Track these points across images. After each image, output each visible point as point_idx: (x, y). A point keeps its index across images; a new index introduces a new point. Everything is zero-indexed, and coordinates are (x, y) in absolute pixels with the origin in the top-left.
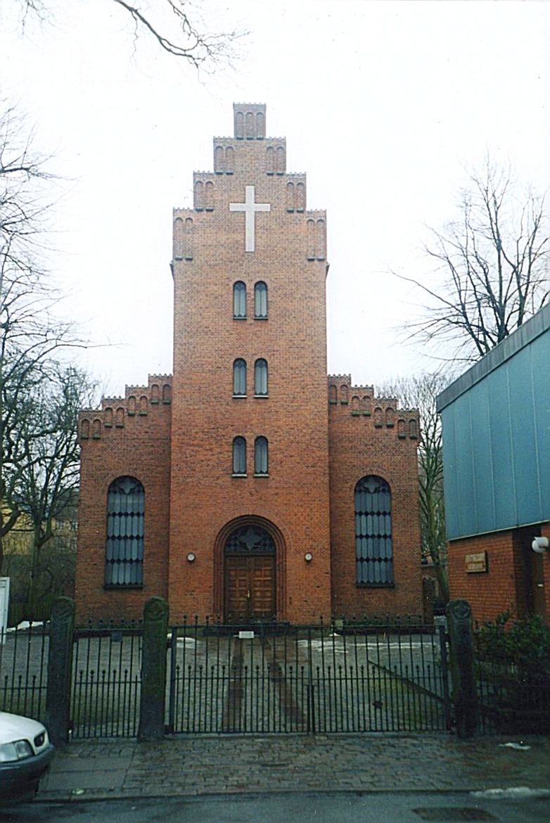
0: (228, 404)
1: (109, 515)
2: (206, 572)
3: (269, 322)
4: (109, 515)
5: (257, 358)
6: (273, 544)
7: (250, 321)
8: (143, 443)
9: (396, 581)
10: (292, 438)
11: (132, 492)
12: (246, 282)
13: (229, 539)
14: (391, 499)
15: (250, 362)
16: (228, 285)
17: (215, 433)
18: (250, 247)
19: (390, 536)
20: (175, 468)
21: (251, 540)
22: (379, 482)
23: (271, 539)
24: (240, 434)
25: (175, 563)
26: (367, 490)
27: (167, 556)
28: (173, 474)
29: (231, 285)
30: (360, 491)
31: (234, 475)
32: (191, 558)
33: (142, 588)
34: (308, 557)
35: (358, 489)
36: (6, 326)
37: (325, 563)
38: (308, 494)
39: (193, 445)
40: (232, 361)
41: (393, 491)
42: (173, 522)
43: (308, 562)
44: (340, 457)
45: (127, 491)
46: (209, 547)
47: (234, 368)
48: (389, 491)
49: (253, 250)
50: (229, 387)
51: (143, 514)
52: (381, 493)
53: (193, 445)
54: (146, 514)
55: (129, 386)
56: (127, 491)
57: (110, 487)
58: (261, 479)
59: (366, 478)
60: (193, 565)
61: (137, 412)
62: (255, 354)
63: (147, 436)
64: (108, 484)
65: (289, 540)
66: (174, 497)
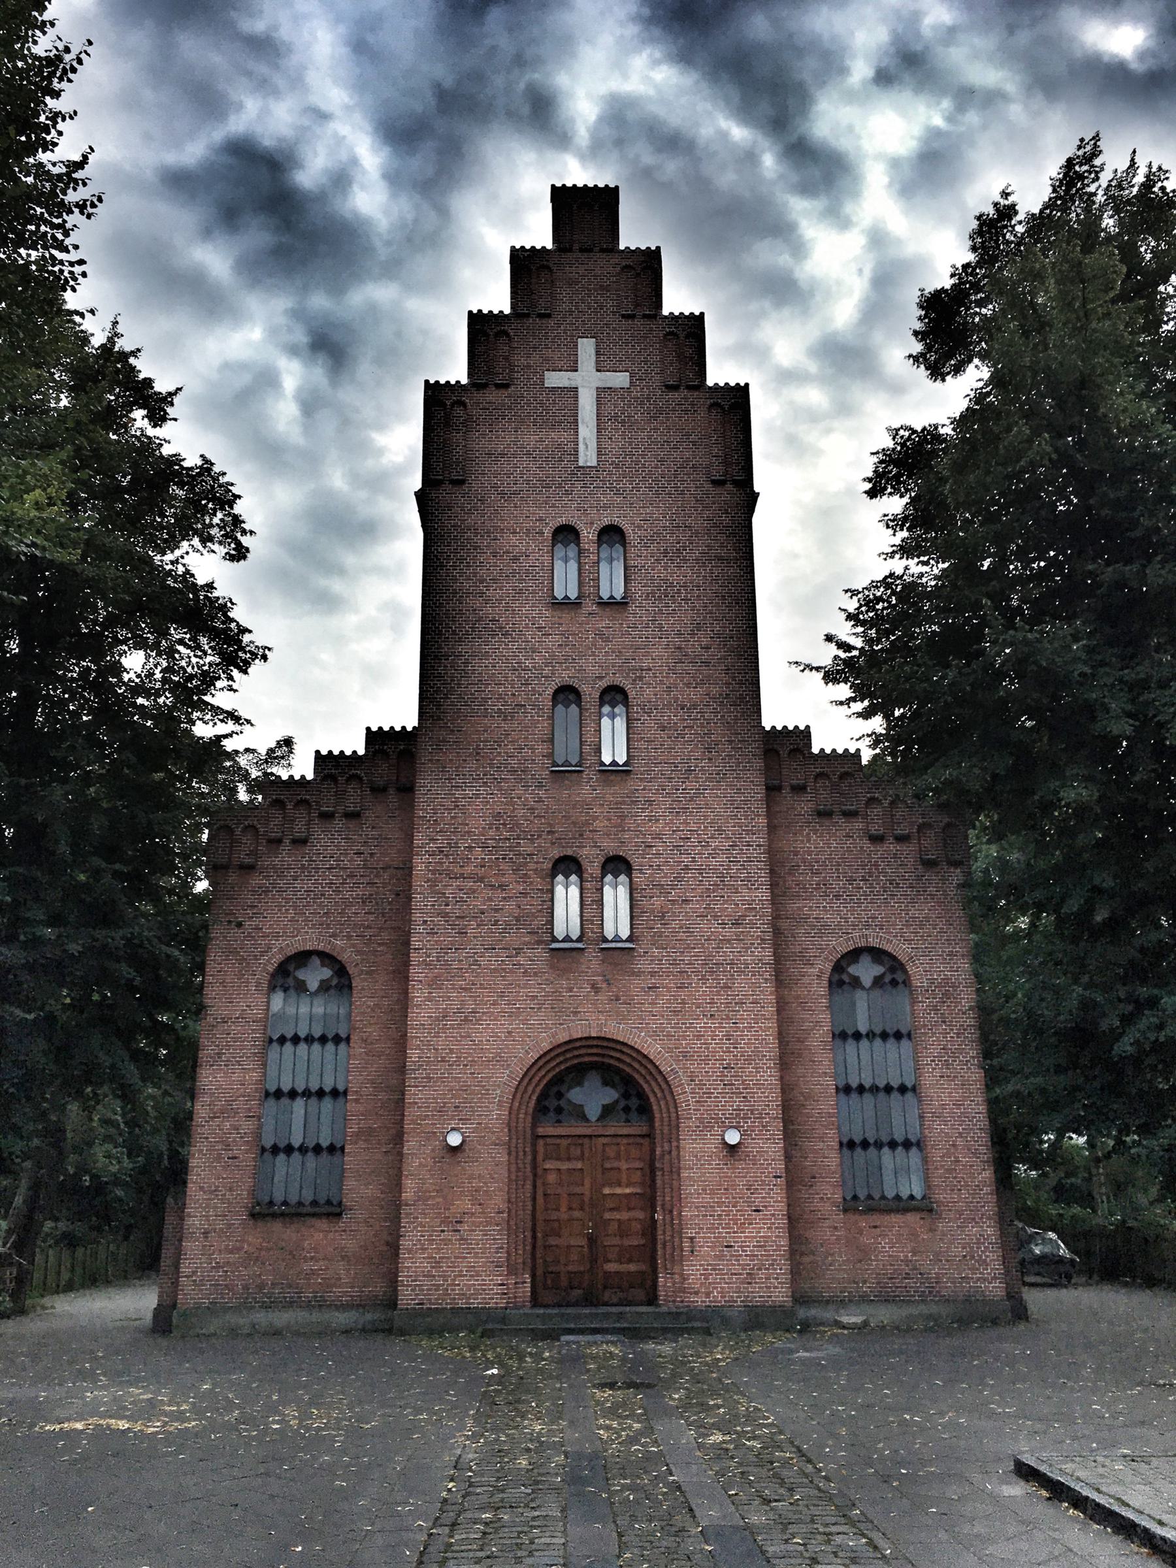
0: (540, 786)
1: (271, 1041)
2: (491, 1170)
3: (632, 608)
4: (271, 1041)
5: (603, 684)
6: (645, 1110)
7: (590, 607)
8: (351, 876)
9: (940, 1196)
10: (686, 860)
11: (325, 987)
12: (580, 526)
13: (544, 1096)
14: (914, 1002)
15: (590, 692)
16: (541, 533)
17: (511, 849)
18: (588, 456)
19: (914, 1089)
20: (421, 929)
21: (592, 1097)
22: (881, 963)
23: (642, 1096)
24: (569, 852)
25: (418, 1156)
26: (856, 983)
27: (398, 1138)
28: (415, 942)
29: (548, 533)
30: (841, 983)
31: (554, 945)
32: (454, 1140)
33: (339, 1215)
34: (733, 1137)
35: (836, 977)
36: (7, 522)
37: (769, 1149)
38: (726, 987)
39: (462, 876)
40: (550, 691)
41: (916, 983)
42: (413, 1055)
43: (733, 1149)
44: (793, 906)
45: (313, 985)
46: (495, 1115)
47: (554, 706)
48: (907, 983)
49: (594, 463)
50: (542, 748)
51: (348, 1039)
52: (889, 987)
53: (462, 876)
54: (354, 1038)
55: (324, 752)
56: (313, 985)
57: (273, 976)
58: (616, 953)
59: (854, 955)
60: (460, 1157)
61: (340, 809)
62: (601, 678)
63: (359, 861)
64: (271, 969)
65: (687, 1098)
66: (418, 994)
